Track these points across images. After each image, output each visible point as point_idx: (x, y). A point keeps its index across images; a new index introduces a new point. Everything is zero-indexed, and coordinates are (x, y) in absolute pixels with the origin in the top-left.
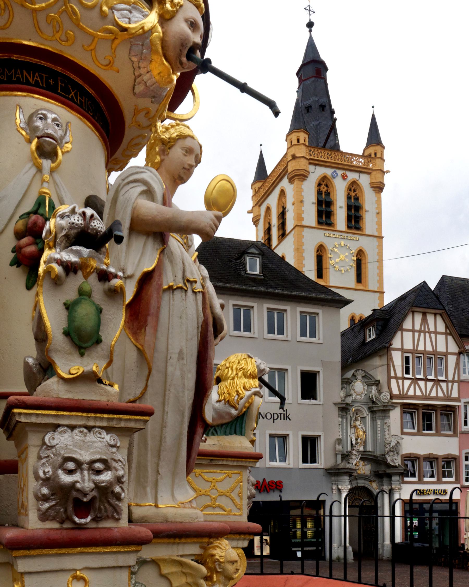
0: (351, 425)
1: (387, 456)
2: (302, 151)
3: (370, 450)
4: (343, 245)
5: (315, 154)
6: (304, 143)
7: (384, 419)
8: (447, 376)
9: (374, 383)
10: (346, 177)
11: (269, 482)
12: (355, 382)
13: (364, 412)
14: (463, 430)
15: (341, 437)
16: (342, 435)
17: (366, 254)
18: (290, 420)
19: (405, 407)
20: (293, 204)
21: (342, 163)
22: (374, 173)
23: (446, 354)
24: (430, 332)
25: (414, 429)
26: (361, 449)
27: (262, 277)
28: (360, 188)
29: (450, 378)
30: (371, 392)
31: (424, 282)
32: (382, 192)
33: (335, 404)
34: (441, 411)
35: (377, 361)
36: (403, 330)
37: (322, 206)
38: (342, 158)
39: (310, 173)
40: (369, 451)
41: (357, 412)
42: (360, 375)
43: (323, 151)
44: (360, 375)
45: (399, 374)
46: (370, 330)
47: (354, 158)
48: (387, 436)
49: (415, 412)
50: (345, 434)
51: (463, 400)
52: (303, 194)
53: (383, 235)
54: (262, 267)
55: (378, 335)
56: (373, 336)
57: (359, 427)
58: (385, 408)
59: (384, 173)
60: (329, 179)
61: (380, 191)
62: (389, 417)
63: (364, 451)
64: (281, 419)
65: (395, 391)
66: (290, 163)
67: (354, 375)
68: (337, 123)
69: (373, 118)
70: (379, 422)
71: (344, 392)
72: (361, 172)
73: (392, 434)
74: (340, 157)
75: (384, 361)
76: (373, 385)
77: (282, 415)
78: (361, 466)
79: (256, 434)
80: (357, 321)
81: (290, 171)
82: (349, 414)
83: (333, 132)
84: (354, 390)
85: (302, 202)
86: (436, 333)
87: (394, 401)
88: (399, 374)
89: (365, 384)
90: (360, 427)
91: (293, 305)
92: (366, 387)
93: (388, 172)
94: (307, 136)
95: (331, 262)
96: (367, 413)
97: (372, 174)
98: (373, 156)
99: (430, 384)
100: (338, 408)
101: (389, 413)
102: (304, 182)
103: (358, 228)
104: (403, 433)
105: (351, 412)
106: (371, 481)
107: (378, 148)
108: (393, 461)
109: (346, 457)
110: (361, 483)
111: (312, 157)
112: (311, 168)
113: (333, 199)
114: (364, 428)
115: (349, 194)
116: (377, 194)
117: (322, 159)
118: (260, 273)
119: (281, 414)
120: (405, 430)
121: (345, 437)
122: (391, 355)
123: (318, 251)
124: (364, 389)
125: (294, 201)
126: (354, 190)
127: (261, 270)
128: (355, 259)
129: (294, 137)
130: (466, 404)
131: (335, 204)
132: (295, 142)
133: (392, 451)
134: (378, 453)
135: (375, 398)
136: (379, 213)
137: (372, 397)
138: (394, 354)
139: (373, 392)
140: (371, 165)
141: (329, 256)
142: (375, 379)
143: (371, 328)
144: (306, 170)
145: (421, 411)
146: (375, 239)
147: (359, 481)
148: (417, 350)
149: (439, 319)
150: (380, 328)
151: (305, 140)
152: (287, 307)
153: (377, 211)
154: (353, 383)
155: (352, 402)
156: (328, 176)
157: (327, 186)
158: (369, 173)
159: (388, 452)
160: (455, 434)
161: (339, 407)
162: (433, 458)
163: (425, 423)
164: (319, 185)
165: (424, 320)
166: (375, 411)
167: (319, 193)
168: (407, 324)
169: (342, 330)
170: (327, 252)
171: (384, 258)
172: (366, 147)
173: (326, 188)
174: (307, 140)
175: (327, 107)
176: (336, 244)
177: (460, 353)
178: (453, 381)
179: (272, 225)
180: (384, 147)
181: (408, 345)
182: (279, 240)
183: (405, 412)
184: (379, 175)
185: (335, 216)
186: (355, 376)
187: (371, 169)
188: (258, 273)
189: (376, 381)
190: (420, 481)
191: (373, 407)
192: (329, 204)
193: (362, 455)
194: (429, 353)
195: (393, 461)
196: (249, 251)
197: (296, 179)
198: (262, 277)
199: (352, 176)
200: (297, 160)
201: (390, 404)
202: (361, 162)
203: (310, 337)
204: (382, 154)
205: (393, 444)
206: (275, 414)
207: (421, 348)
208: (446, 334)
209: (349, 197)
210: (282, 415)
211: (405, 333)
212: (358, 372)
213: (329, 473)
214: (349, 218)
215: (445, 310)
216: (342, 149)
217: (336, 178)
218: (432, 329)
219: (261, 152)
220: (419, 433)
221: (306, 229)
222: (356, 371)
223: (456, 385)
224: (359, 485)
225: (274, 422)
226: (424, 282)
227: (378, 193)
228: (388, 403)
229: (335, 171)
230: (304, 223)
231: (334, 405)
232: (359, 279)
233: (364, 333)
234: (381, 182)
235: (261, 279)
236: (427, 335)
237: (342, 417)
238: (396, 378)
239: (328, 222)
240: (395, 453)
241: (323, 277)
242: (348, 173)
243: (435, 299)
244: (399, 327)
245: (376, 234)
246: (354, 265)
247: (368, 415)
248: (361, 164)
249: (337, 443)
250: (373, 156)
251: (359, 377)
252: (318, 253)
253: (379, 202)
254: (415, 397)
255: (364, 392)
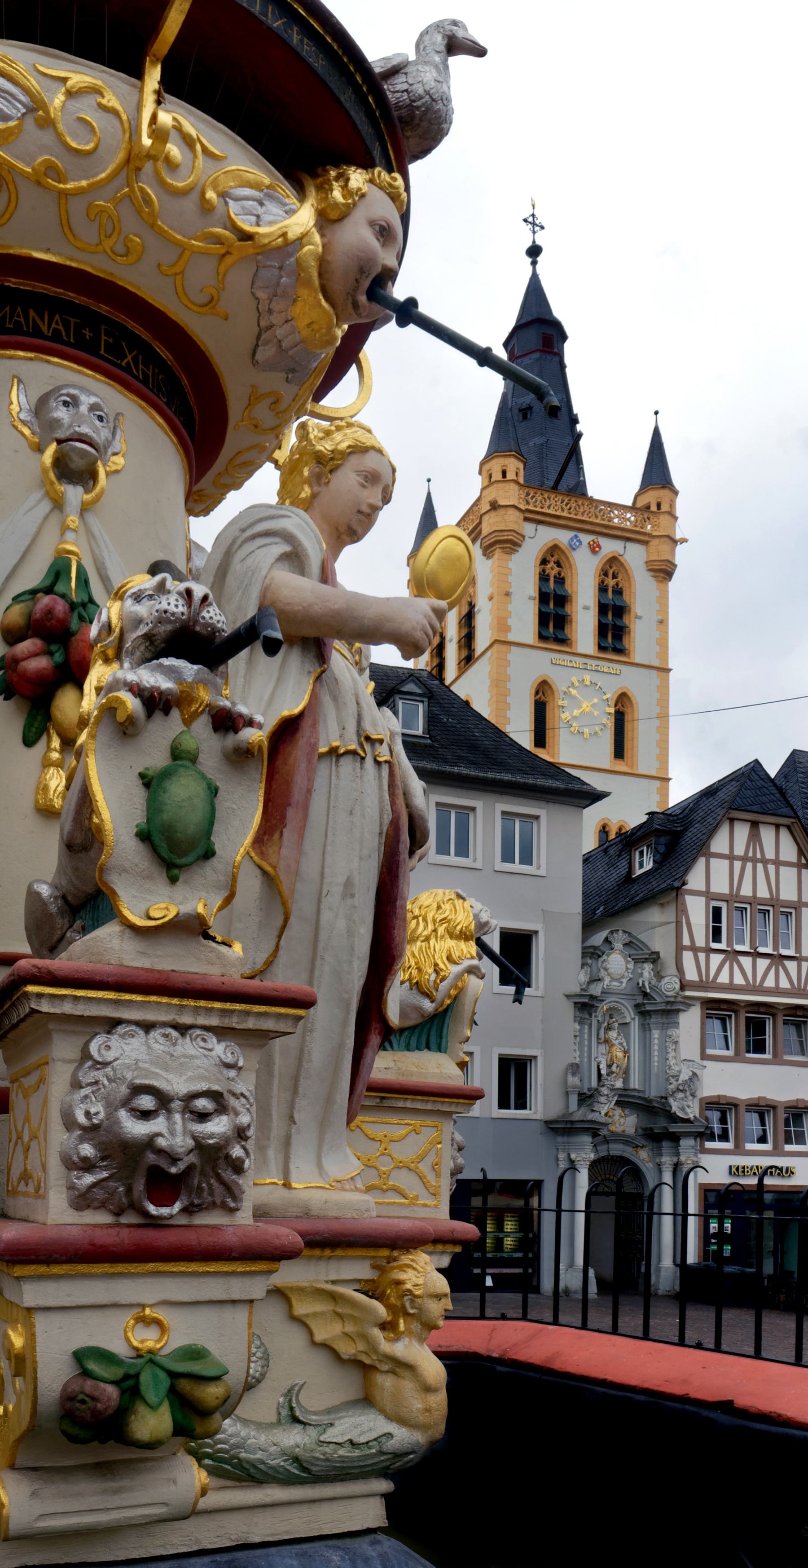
0: (598, 1038)
1: (671, 1100)
2: (510, 495)
3: (637, 1087)
4: (588, 683)
5: (536, 501)
6: (515, 478)
7: (667, 1028)
9: (647, 956)
10: (597, 549)
12: (608, 955)
13: (626, 1014)
15: (577, 1060)
16: (579, 1057)
17: (634, 702)
19: (709, 1006)
20: (491, 598)
21: (591, 520)
22: (654, 543)
24: (765, 862)
25: (728, 1049)
26: (619, 1084)
27: (429, 741)
28: (626, 571)
30: (641, 975)
31: (757, 762)
32: (670, 580)
33: (568, 996)
34: (785, 1016)
35: (654, 915)
36: (709, 855)
37: (548, 603)
38: (592, 510)
39: (526, 538)
40: (635, 1090)
41: (612, 1012)
42: (619, 942)
43: (553, 496)
44: (619, 942)
45: (700, 942)
46: (641, 853)
47: (616, 512)
48: (672, 1062)
49: (730, 1016)
50: (586, 1055)
52: (510, 579)
53: (670, 667)
54: (429, 721)
55: (659, 864)
56: (648, 865)
57: (614, 1042)
58: (669, 1008)
59: (675, 542)
60: (563, 552)
61: (665, 579)
62: (676, 1025)
63: (625, 1090)
65: (691, 974)
66: (486, 518)
67: (607, 941)
68: (583, 443)
69: (656, 434)
70: (656, 1034)
71: (586, 973)
72: (628, 539)
73: (683, 1058)
74: (586, 508)
75: (670, 914)
76: (646, 960)
78: (617, 1117)
80: (612, 836)
81: (485, 532)
82: (596, 1016)
83: (574, 458)
84: (606, 970)
85: (508, 594)
86: (778, 863)
87: (688, 993)
88: (700, 942)
89: (629, 959)
90: (616, 1042)
91: (490, 798)
92: (631, 966)
93: (684, 541)
94: (521, 466)
95: (563, 716)
96: (633, 1016)
97: (651, 543)
98: (654, 508)
99: (763, 964)
100: (573, 1004)
101: (677, 1018)
102: (513, 556)
103: (620, 651)
104: (704, 1056)
105: (599, 1014)
106: (637, 1146)
107: (664, 494)
108: (683, 1109)
109: (586, 1098)
110: (617, 1149)
111: (531, 507)
112: (529, 529)
113: (570, 592)
114: (625, 1044)
115: (603, 582)
116: (660, 584)
117: (551, 511)
118: (423, 733)
120: (709, 1052)
121: (586, 1060)
122: (684, 904)
123: (537, 693)
124: (627, 968)
125: (492, 593)
126: (613, 573)
127: (426, 727)
128: (612, 710)
129: (496, 466)
131: (574, 600)
132: (498, 476)
133: (682, 1091)
134: (653, 1093)
135: (650, 988)
136: (663, 622)
137: (643, 985)
138: (690, 900)
139: (646, 974)
140: (649, 527)
141: (560, 703)
142: (649, 949)
143: (645, 849)
144: (517, 533)
145: (743, 1016)
146: (654, 673)
147: (611, 1146)
148: (737, 895)
149: (785, 835)
150: (662, 849)
151: (517, 474)
152: (478, 802)
153: (660, 617)
154: (605, 957)
155: (602, 993)
156: (561, 546)
157: (558, 564)
158: (645, 543)
159: (674, 1092)
161: (575, 1003)
162: (767, 1106)
163: (752, 1038)
164: (544, 562)
165: (754, 837)
166: (648, 1012)
167: (543, 578)
168: (719, 843)
169: (585, 851)
170: (556, 696)
171: (673, 709)
172: (640, 490)
173: (557, 569)
174: (522, 473)
175: (564, 410)
176: (574, 679)
179: (448, 638)
180: (676, 493)
181: (721, 886)
182: (460, 669)
183: (709, 1016)
184: (665, 547)
185: (574, 624)
186: (610, 943)
187: (649, 535)
188: (420, 732)
189: (653, 953)
190: (738, 1150)
191: (644, 1004)
192: (562, 600)
193: (620, 1096)
194: (763, 902)
195: (683, 1109)
196: (404, 689)
197: (498, 550)
198: (429, 741)
199: (609, 547)
200: (501, 512)
201: (680, 999)
202: (629, 520)
203: (521, 863)
204: (672, 505)
205: (684, 1076)
207: (746, 891)
209: (602, 589)
211: (713, 861)
212: (615, 935)
213: (552, 1129)
214: (602, 631)
215: (798, 818)
216: (590, 493)
217: (578, 550)
218: (770, 854)
219: (429, 494)
220: (737, 1058)
221: (514, 649)
222: (612, 932)
224: (612, 1153)
226: (757, 762)
227: (661, 582)
228: (675, 997)
229: (576, 536)
230: (511, 637)
231: (565, 999)
232: (619, 752)
233: (630, 859)
234: (668, 561)
235: (426, 746)
236: (760, 866)
237: (581, 1022)
238: (694, 949)
239: (560, 637)
240: (688, 1093)
241: (547, 745)
242: (602, 541)
243: (778, 795)
244: (702, 848)
245: (656, 663)
246: (610, 723)
247: (633, 1019)
248: (628, 523)
249: (570, 1071)
250: (654, 508)
251: (618, 945)
252: (538, 697)
253: (663, 600)
254: (731, 987)
255: (626, 974)
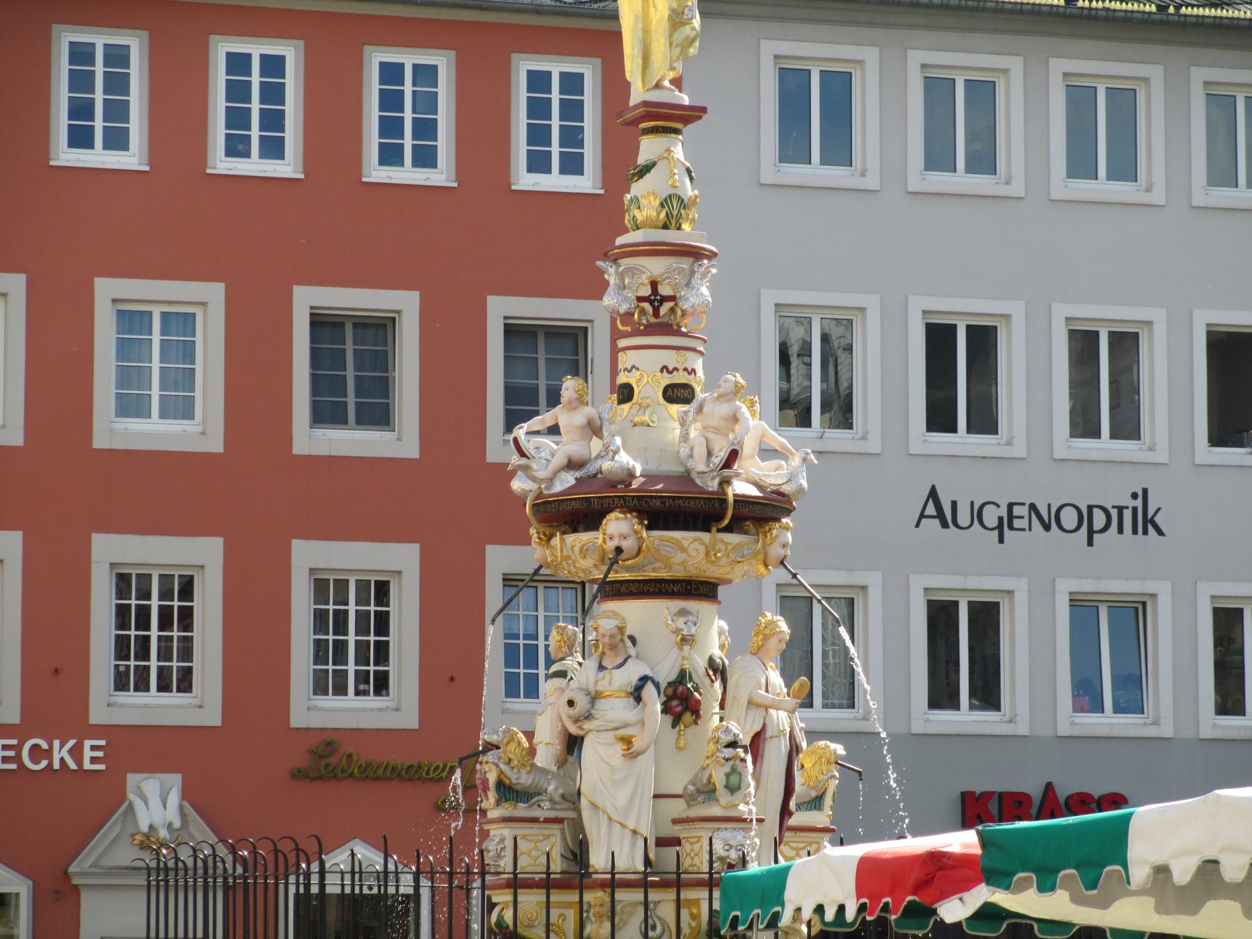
18: (1160, 533)
64: (1120, 531)
77: (1128, 515)
206: (1096, 511)
210: (1128, 515)
225: (1090, 543)
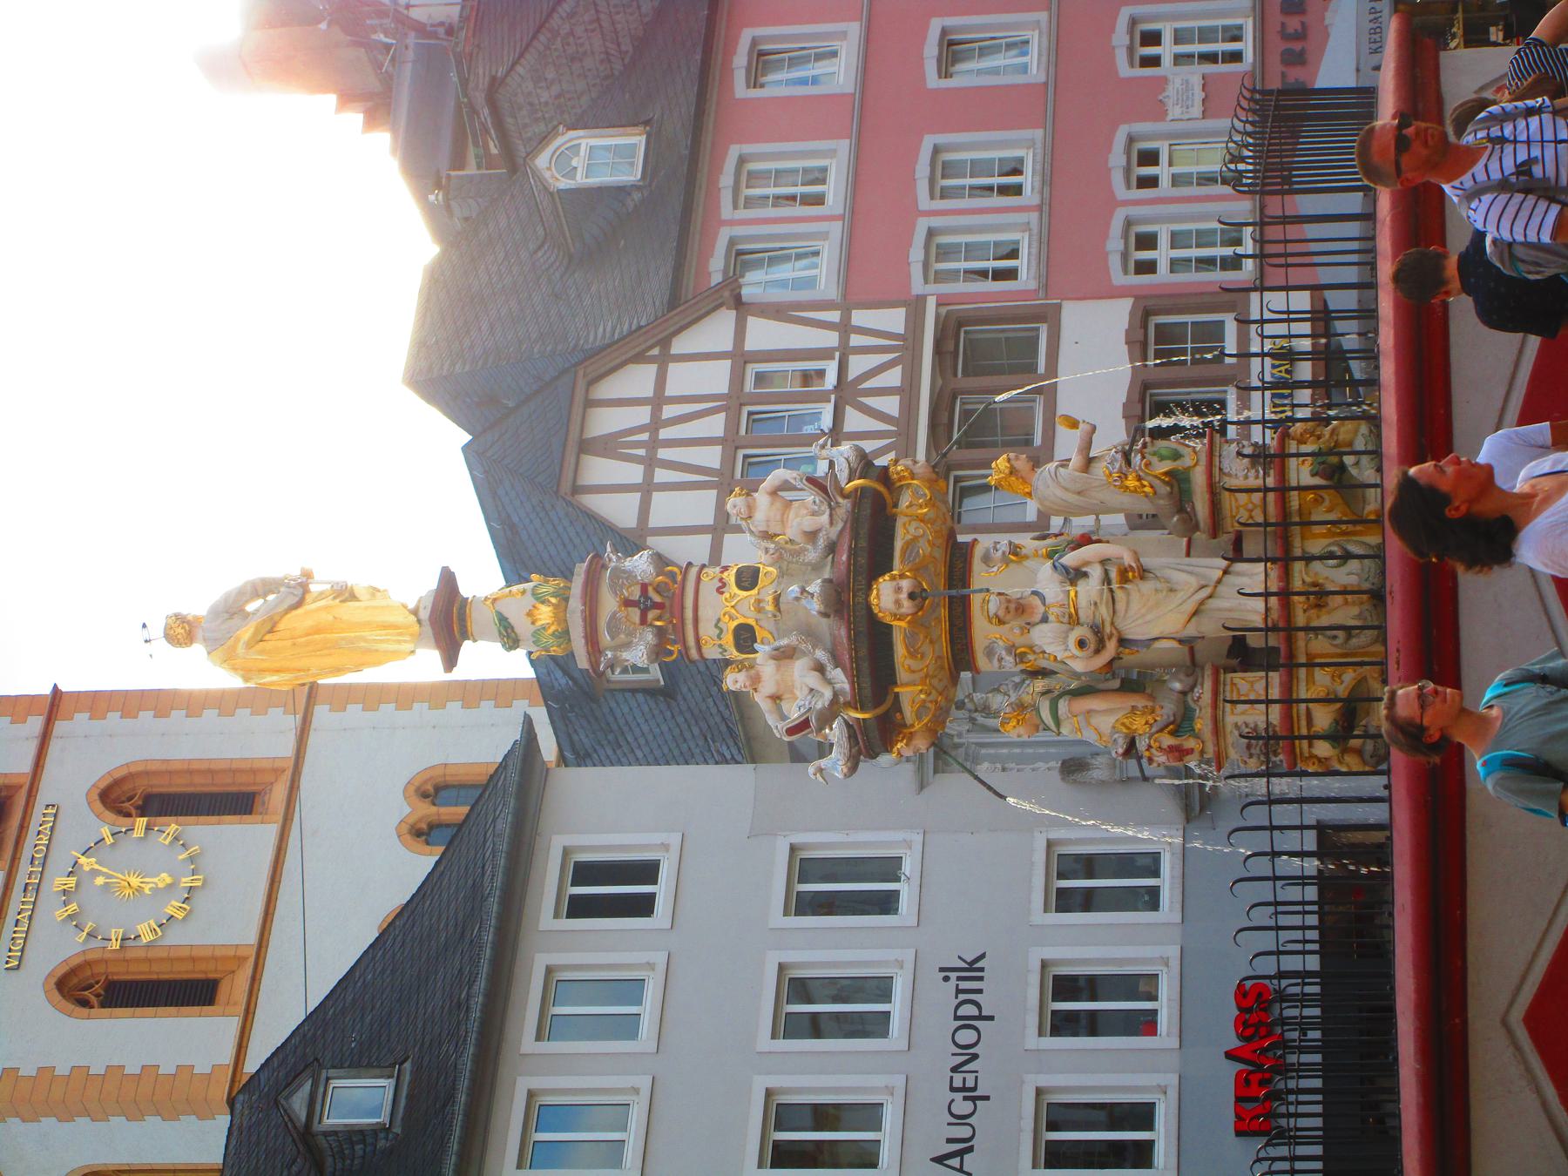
8: (825, 354)
11: (1240, 1036)
14: (1032, 285)
18: (983, 956)
23: (740, 358)
24: (656, 423)
29: (831, 339)
33: (922, 786)
51: (918, 286)
77: (964, 985)
79: (1040, 1084)
86: (658, 400)
119: (959, 991)
130: (932, 277)
160: (1051, 316)
161: (935, 772)
177: (738, 303)
178: (845, 328)
208: (664, 360)
210: (964, 985)
223: (860, 318)
225: (991, 1018)
231: (925, 791)
249: (1078, 776)
